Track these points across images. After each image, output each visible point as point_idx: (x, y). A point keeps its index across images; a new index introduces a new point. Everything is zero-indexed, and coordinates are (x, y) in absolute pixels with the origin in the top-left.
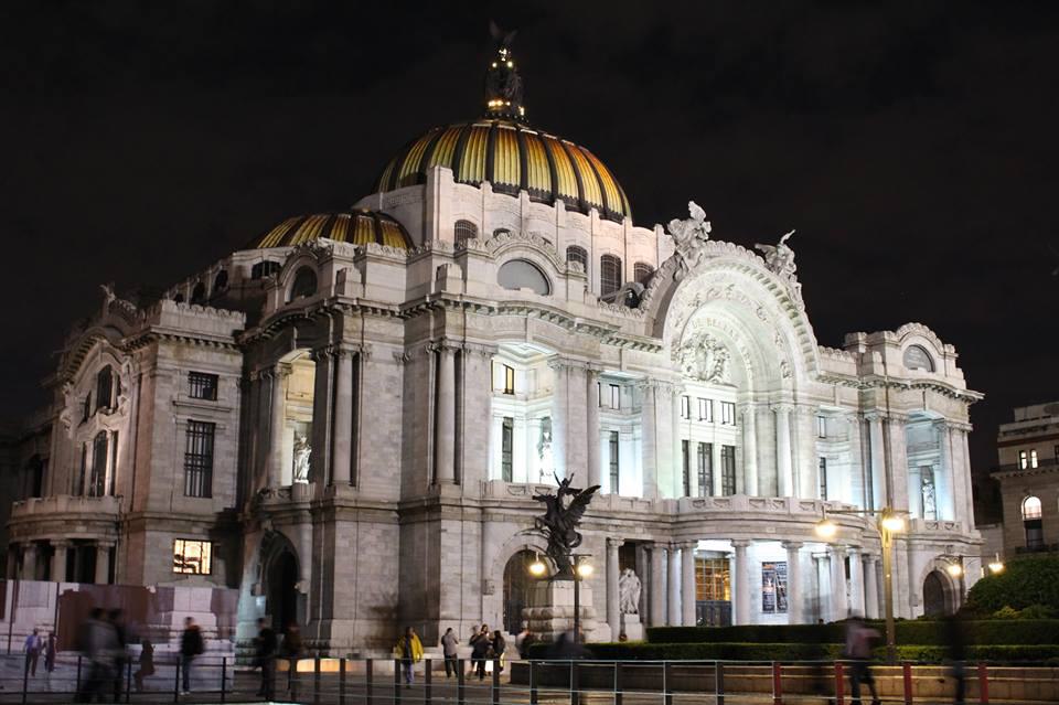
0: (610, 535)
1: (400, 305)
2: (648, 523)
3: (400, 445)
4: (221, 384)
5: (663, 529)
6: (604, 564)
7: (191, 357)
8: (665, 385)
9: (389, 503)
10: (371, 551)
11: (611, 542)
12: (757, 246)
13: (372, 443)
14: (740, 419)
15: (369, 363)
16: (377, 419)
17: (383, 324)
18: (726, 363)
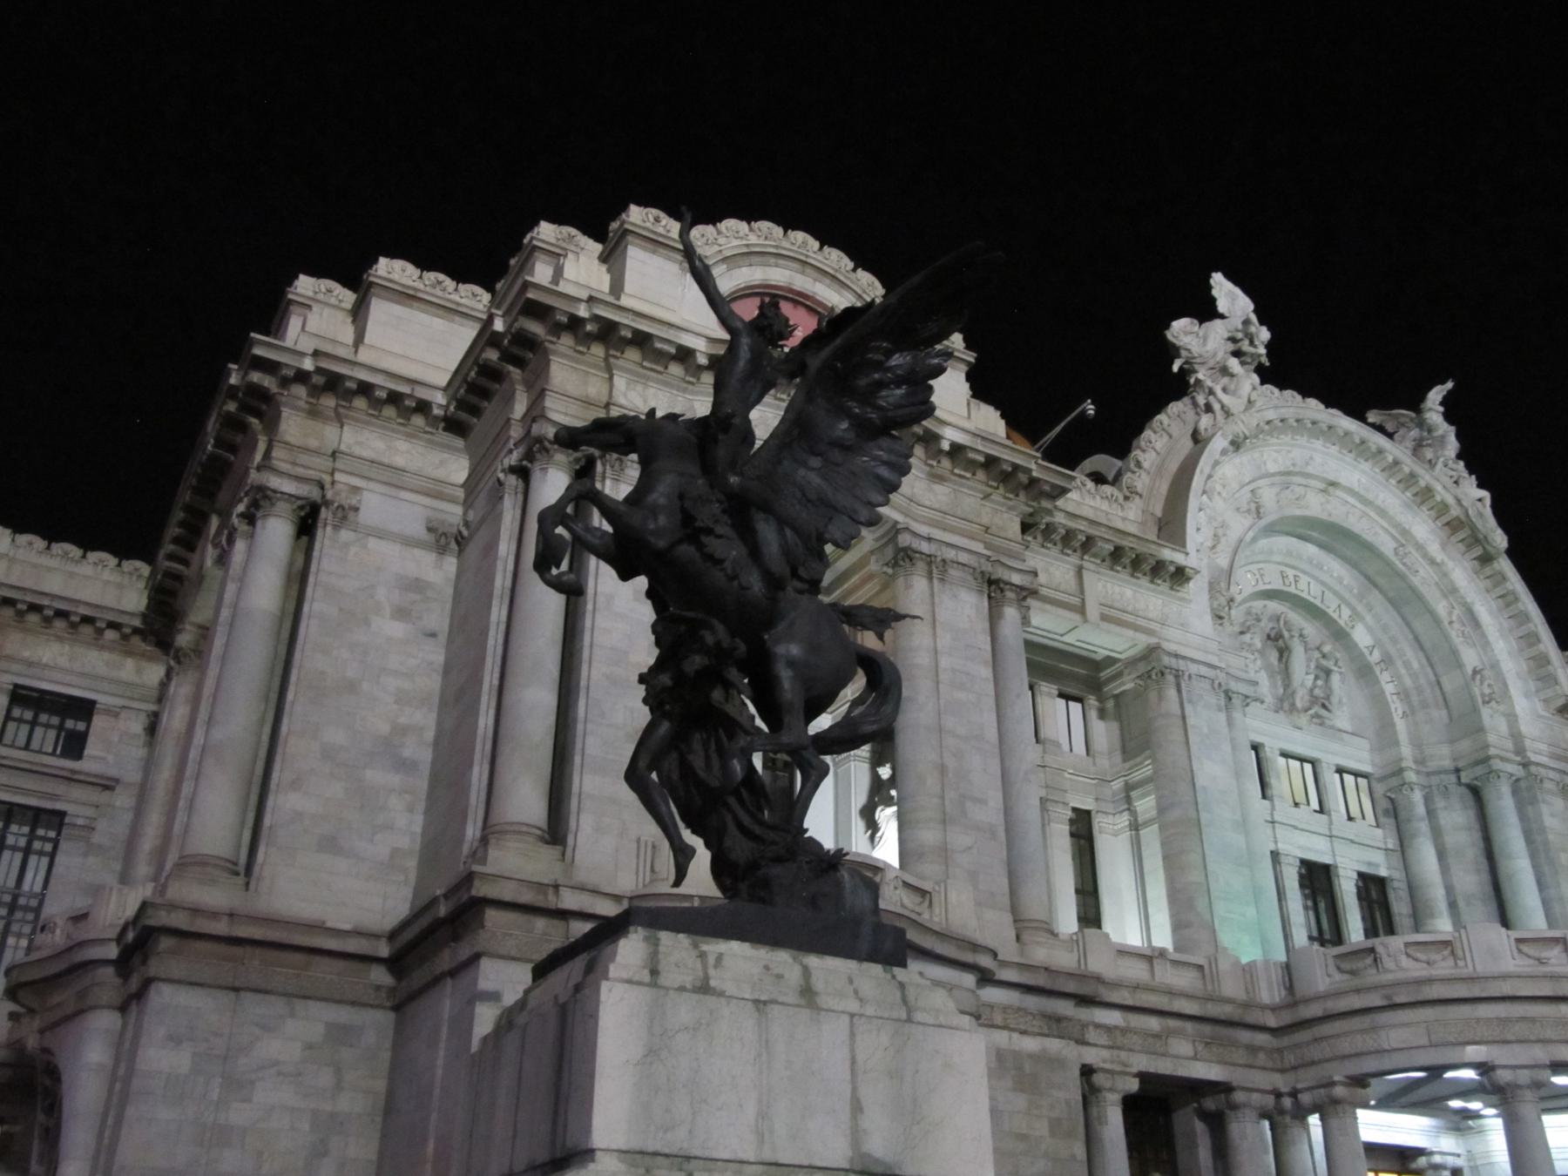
0: (1092, 1056)
1: (445, 390)
2: (1207, 1029)
3: (425, 770)
4: (98, 722)
5: (1252, 1049)
6: (1079, 1150)
7: (26, 654)
8: (1204, 670)
9: (357, 933)
10: (270, 1093)
11: (1098, 1079)
12: (1372, 417)
13: (328, 753)
14: (1393, 812)
15: (345, 535)
16: (352, 687)
17: (402, 445)
18: (1335, 679)
